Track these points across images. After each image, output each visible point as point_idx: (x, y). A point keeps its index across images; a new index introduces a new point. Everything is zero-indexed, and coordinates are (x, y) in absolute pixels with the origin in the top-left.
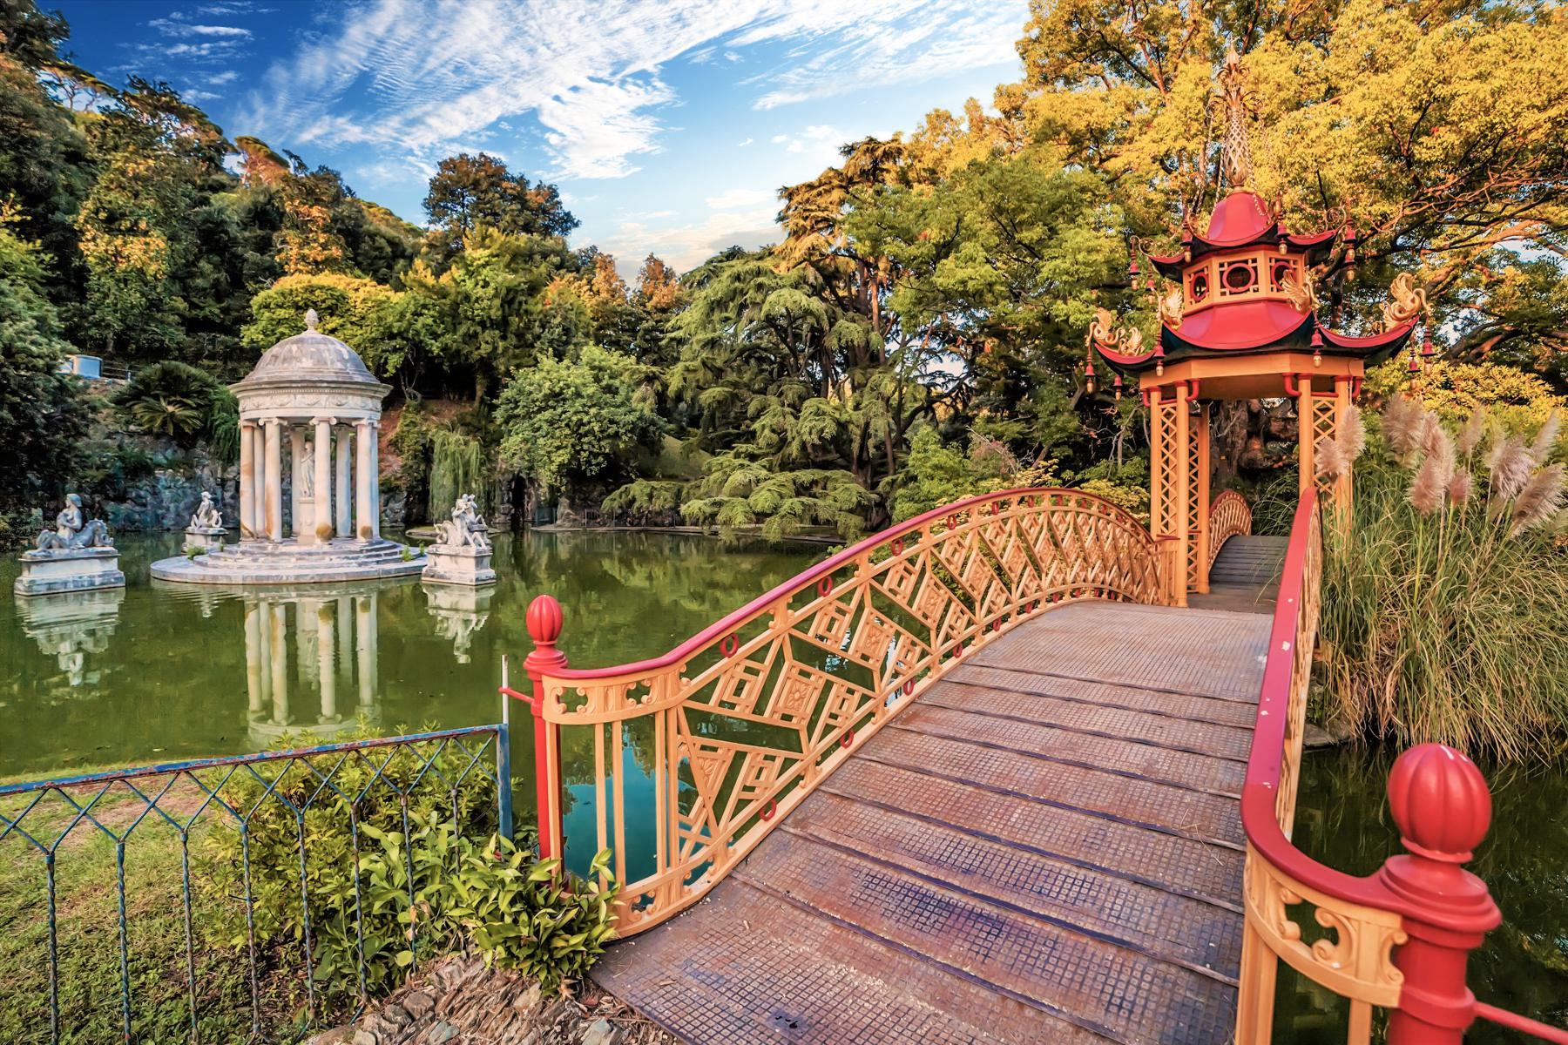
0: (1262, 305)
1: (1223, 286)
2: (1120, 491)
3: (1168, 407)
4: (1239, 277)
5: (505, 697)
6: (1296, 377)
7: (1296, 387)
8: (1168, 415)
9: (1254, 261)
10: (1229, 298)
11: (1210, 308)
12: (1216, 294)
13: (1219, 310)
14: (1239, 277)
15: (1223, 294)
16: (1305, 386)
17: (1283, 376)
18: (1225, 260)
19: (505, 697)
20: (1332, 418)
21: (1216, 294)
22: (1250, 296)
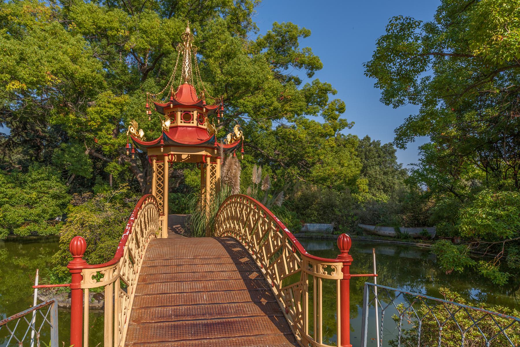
0: (194, 128)
1: (181, 119)
2: (239, 178)
3: (160, 164)
4: (187, 117)
5: (376, 287)
6: (206, 156)
7: (206, 160)
8: (160, 167)
9: (193, 112)
10: (183, 124)
11: (177, 127)
12: (179, 122)
13: (180, 128)
14: (187, 117)
15: (181, 122)
16: (208, 159)
17: (202, 155)
18: (183, 110)
19: (376, 287)
20: (215, 171)
21: (179, 122)
22: (191, 125)
